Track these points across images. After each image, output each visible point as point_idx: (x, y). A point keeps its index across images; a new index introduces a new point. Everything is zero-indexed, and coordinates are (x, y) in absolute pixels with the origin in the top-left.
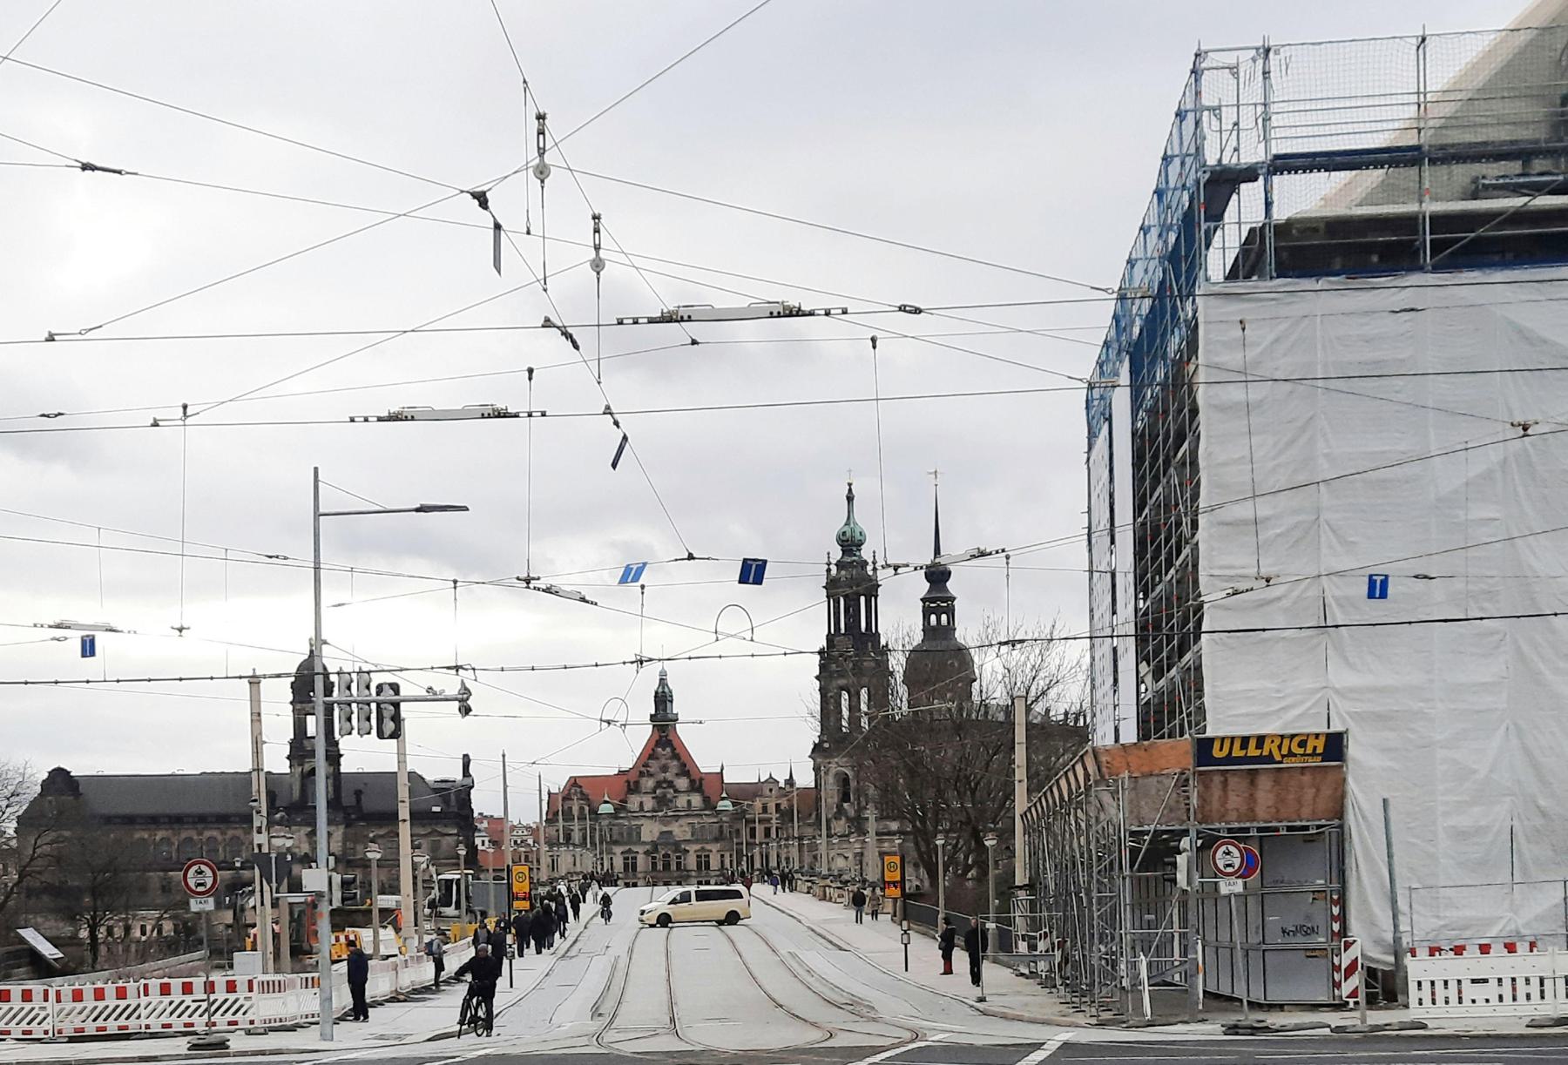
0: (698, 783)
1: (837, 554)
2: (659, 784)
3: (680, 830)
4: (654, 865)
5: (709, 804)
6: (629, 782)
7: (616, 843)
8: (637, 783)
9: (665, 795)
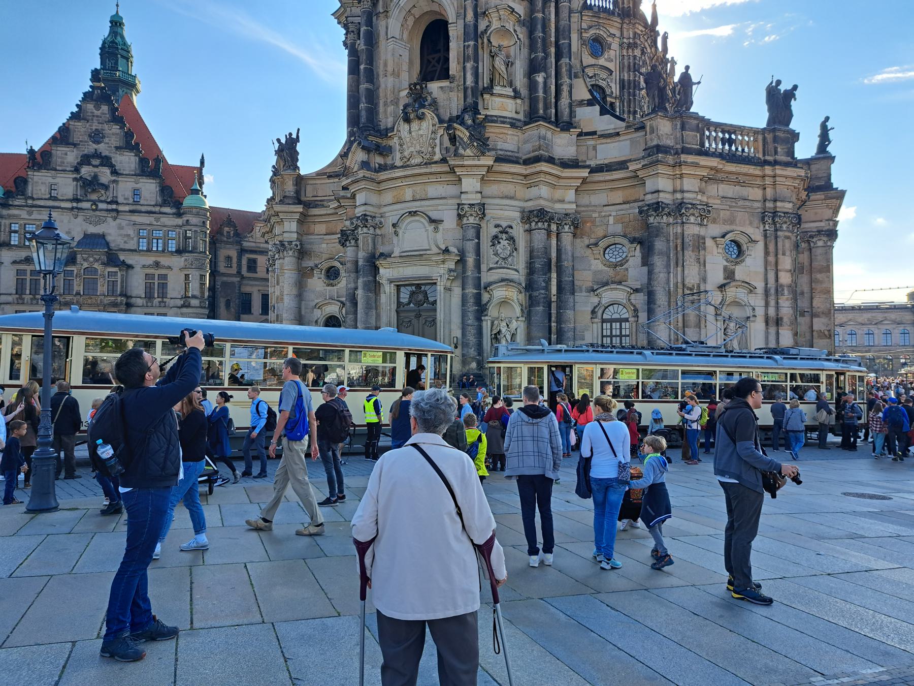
0: (152, 165)
2: (86, 160)
3: (114, 231)
9: (95, 177)
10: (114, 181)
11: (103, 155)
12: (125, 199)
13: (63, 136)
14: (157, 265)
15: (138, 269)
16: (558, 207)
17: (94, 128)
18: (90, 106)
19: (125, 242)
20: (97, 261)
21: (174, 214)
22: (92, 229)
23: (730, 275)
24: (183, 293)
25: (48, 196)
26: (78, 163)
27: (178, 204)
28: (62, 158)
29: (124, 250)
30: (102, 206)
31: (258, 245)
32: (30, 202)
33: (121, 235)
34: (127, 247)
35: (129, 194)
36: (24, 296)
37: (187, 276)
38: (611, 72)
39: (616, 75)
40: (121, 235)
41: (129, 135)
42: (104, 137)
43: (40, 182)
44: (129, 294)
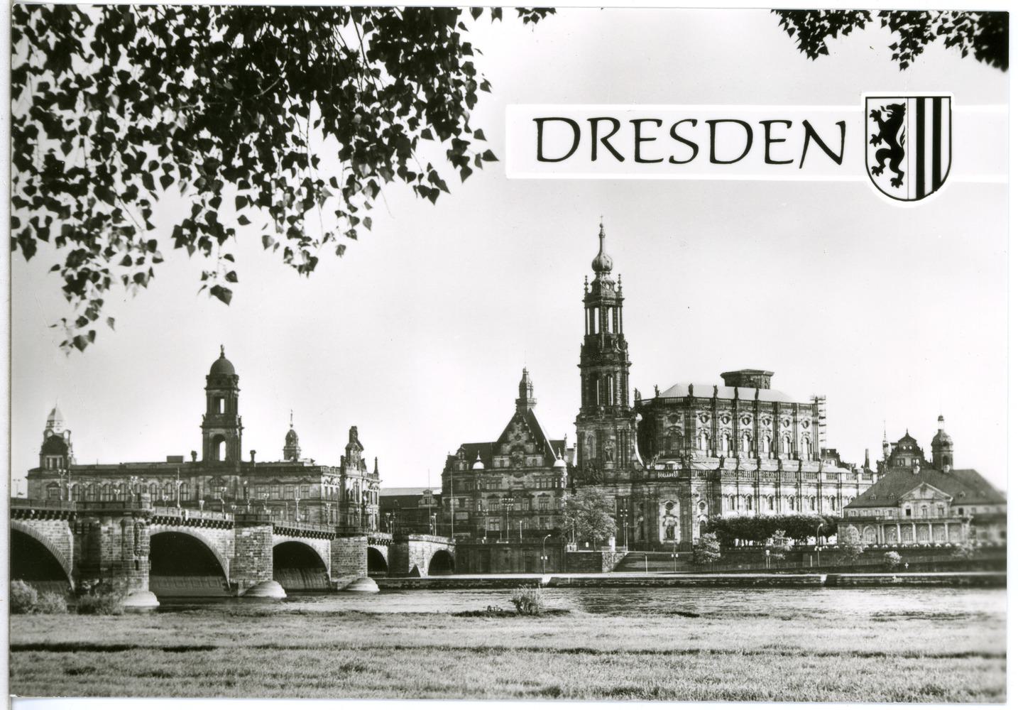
1: (592, 276)
2: (514, 449)
7: (485, 490)
13: (504, 438)
16: (627, 494)
22: (517, 480)
23: (668, 513)
35: (531, 462)
38: (679, 428)
39: (683, 427)
43: (497, 461)
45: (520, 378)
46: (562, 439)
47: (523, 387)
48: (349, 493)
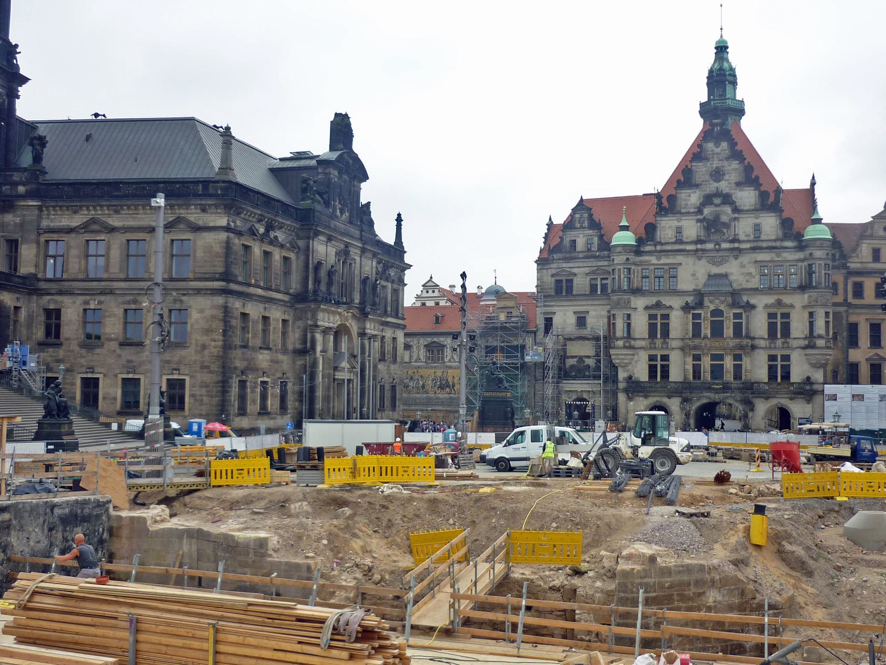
0: (771, 198)
2: (708, 200)
3: (740, 272)
4: (697, 328)
5: (791, 231)
6: (664, 203)
7: (637, 291)
8: (672, 199)
9: (717, 217)
10: (735, 219)
11: (724, 192)
12: (747, 236)
13: (684, 177)
14: (779, 303)
15: (760, 308)
17: (715, 166)
18: (710, 146)
19: (747, 281)
20: (723, 302)
21: (795, 248)
22: (715, 270)
24: (807, 332)
25: (674, 240)
26: (701, 204)
27: (799, 236)
28: (685, 200)
29: (747, 290)
30: (725, 245)
31: (865, 265)
32: (659, 248)
33: (743, 274)
34: (750, 286)
35: (750, 230)
36: (656, 341)
37: (811, 314)
40: (743, 274)
41: (748, 169)
42: (724, 174)
43: (667, 227)
44: (752, 335)
45: (709, 59)
46: (808, 186)
47: (721, 78)
48: (323, 274)
